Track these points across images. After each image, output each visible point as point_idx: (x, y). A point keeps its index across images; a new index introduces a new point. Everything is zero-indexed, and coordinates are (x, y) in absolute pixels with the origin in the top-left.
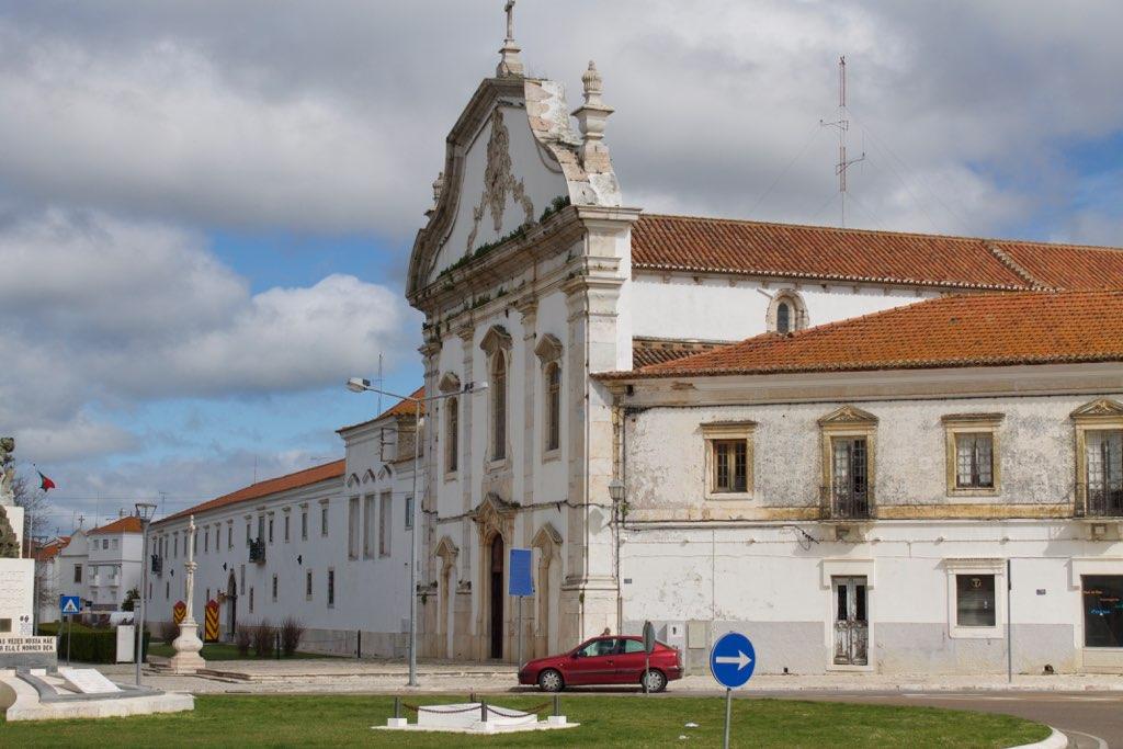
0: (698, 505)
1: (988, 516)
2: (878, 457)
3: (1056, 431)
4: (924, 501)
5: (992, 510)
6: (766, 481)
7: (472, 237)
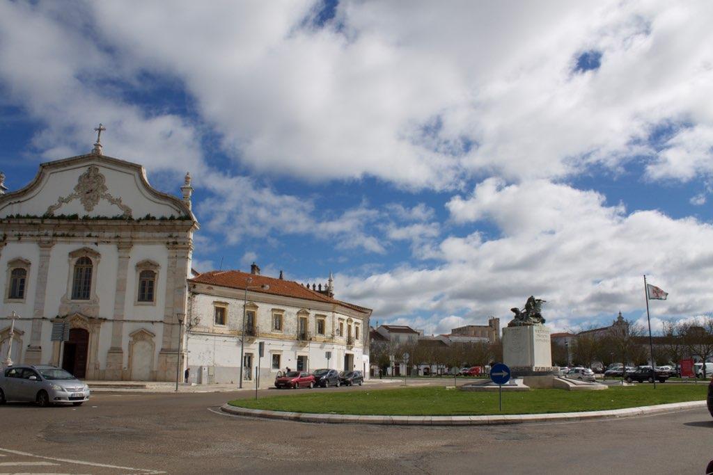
0: (211, 328)
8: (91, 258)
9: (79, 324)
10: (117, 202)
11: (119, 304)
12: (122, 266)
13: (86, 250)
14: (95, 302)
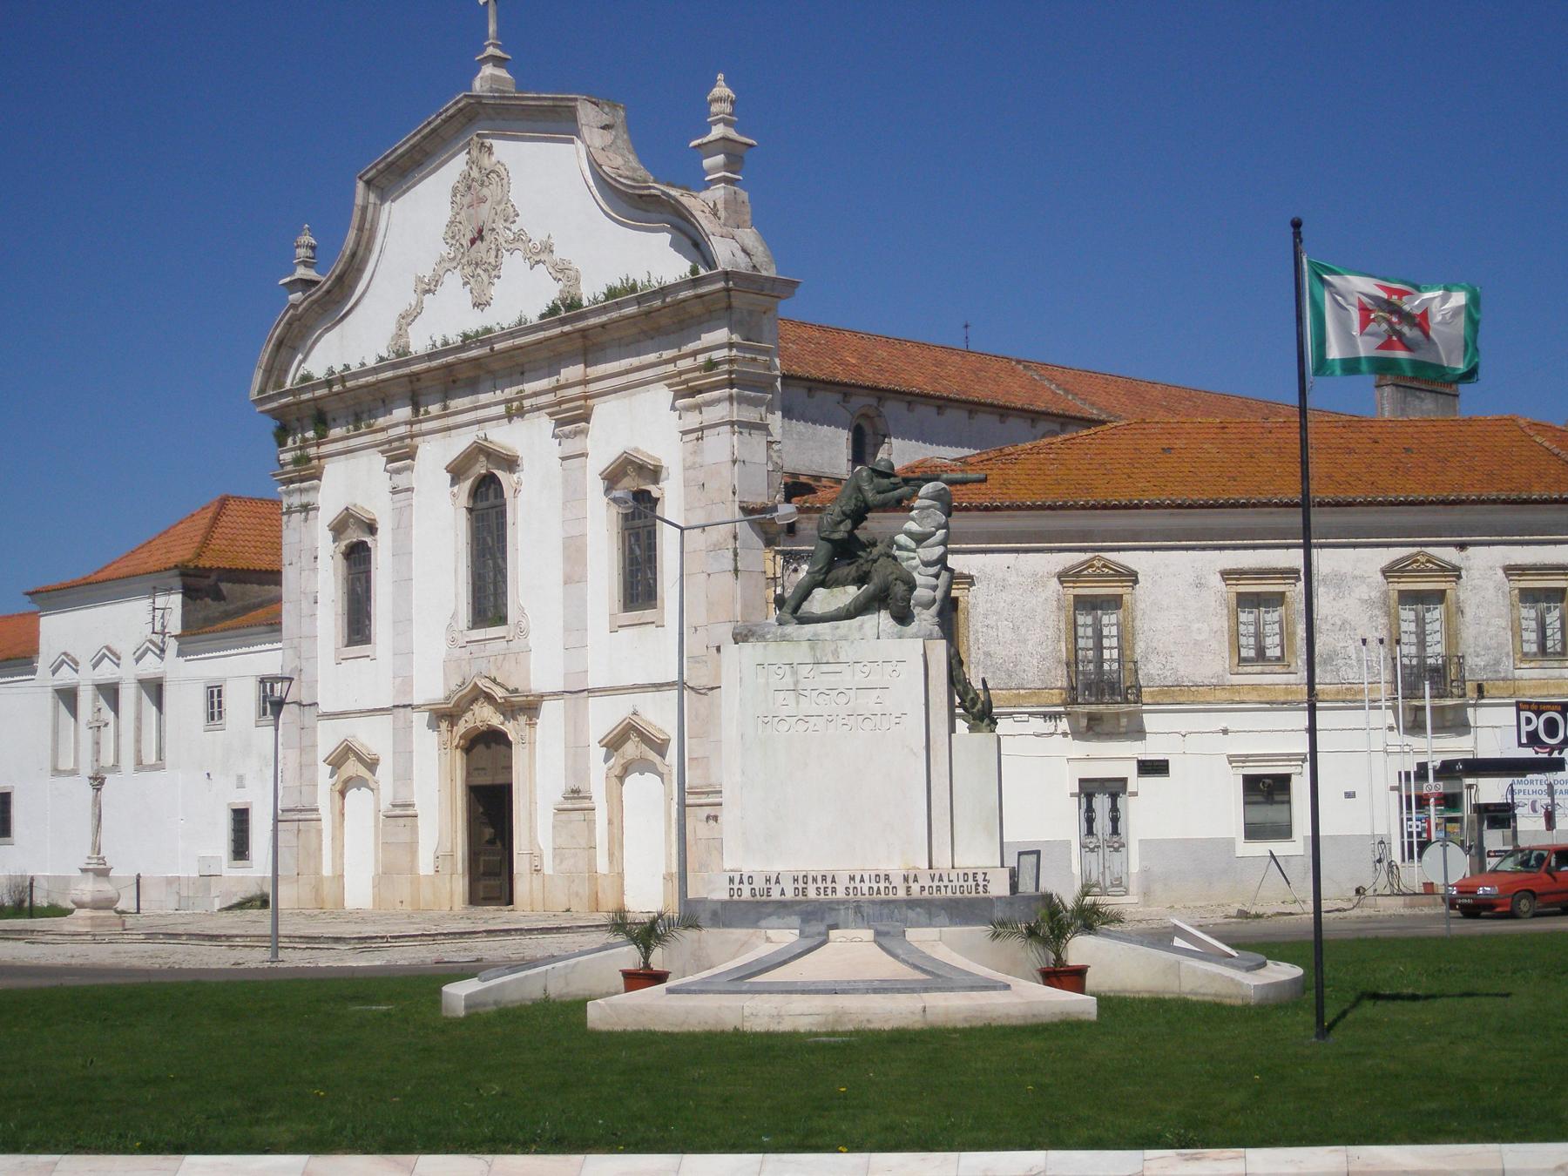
1: (1282, 699)
2: (1138, 623)
3: (1363, 592)
4: (1199, 680)
5: (1287, 692)
6: (987, 654)
7: (408, 318)
8: (496, 472)
9: (485, 716)
10: (540, 254)
11: (575, 627)
12: (573, 496)
13: (480, 450)
14: (523, 632)
